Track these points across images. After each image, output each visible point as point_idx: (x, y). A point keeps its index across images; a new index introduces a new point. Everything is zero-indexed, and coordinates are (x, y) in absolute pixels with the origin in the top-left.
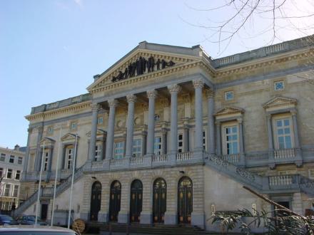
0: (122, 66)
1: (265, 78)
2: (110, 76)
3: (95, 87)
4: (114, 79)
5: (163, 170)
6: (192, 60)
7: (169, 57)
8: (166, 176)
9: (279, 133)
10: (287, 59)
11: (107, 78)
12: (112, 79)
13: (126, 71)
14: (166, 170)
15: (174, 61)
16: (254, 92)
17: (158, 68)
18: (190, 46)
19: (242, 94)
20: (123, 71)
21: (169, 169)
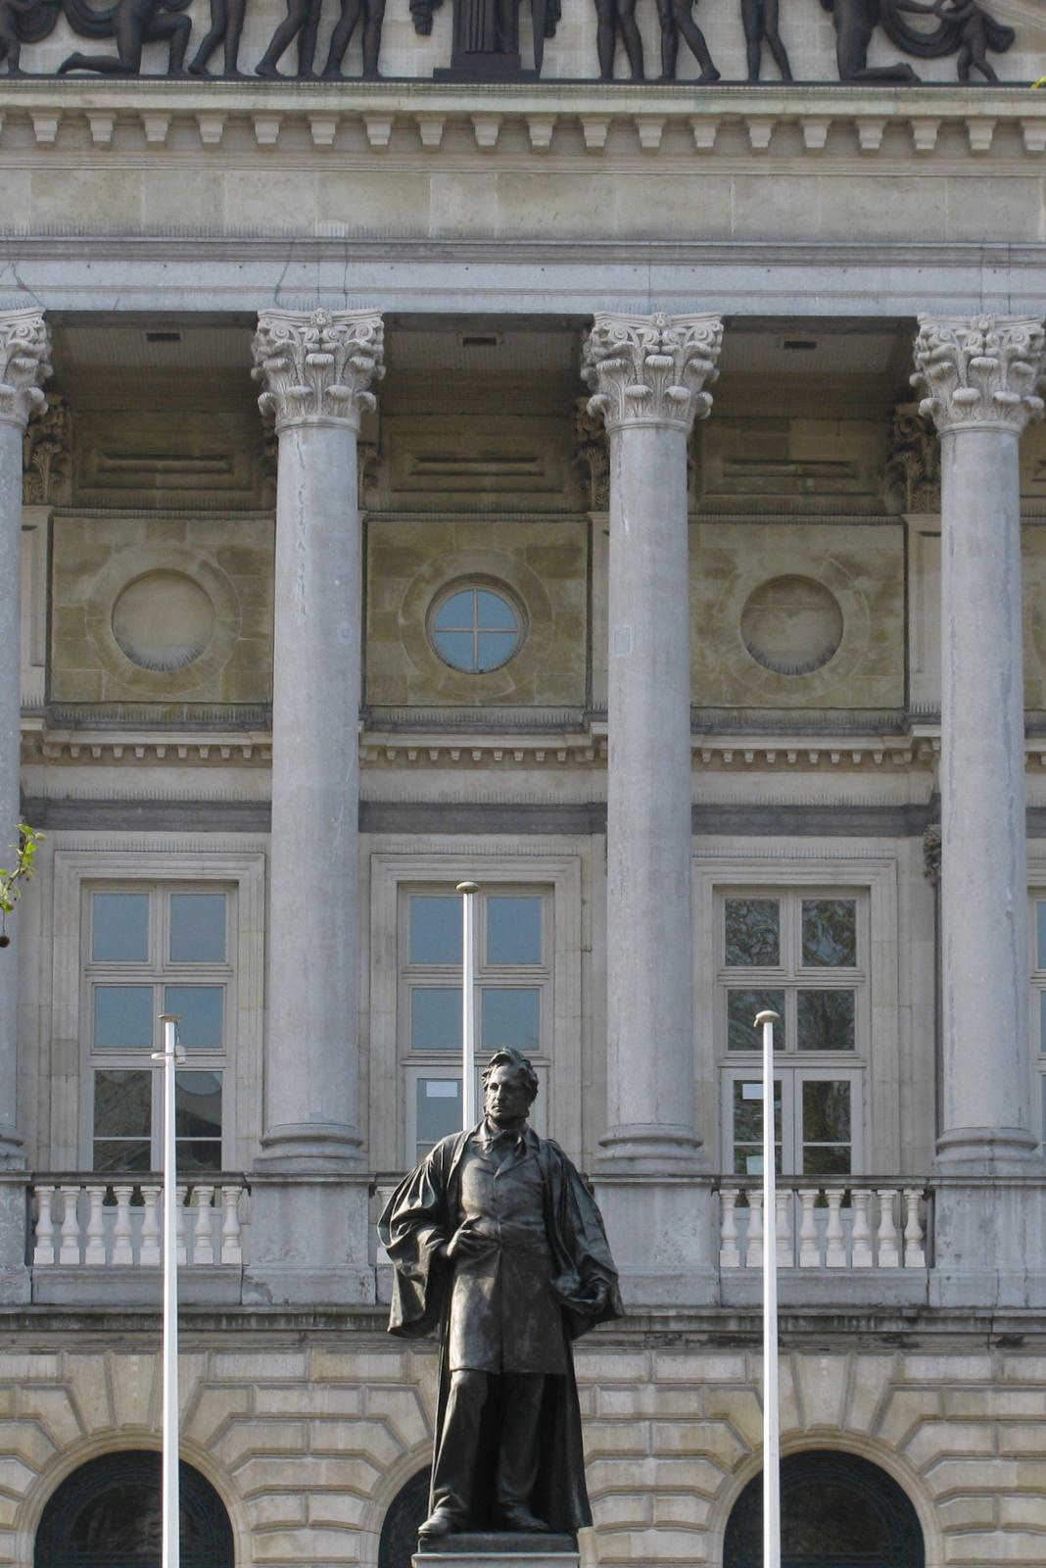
5: (874, 1370)
8: (934, 1438)
14: (919, 1367)
21: (975, 1367)
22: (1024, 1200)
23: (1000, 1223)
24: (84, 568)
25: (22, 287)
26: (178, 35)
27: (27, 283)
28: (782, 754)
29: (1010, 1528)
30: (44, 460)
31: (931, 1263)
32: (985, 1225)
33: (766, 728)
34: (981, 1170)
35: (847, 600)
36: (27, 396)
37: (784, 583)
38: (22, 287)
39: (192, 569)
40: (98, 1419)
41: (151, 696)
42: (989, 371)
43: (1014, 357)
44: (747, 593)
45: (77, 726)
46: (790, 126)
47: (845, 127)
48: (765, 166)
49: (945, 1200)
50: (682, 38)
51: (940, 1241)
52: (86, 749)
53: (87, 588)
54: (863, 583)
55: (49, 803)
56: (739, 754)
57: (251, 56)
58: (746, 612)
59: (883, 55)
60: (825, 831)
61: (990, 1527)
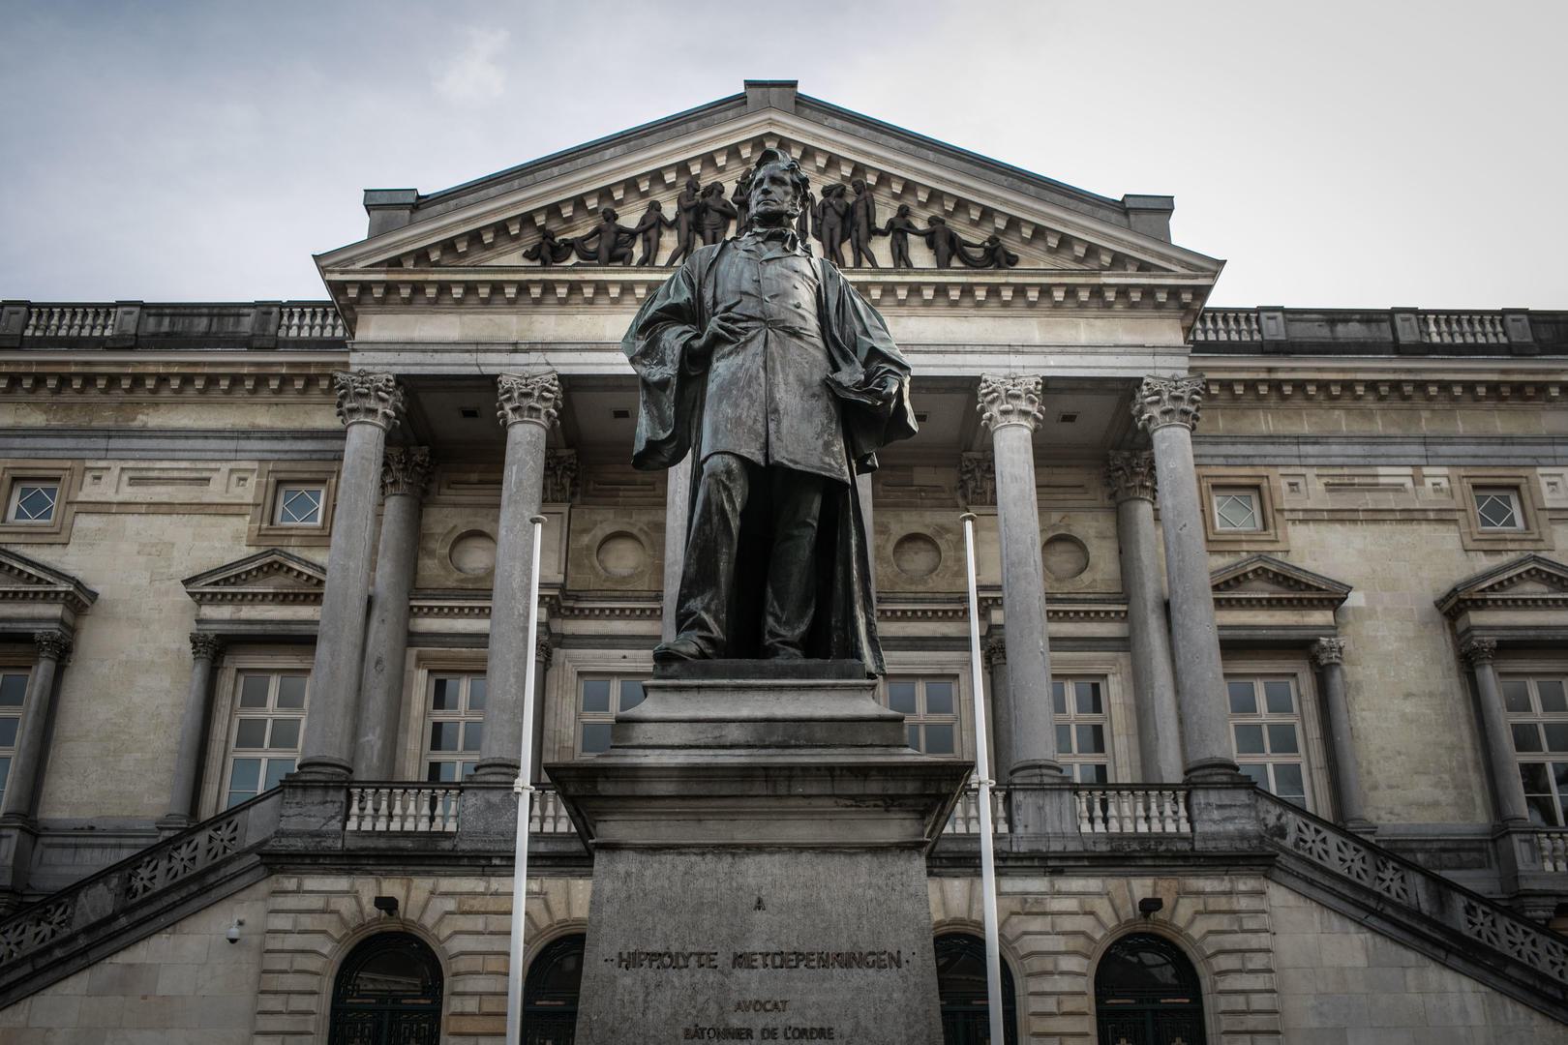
0: (631, 185)
1: (1430, 460)
2: (527, 219)
3: (395, 263)
4: (549, 252)
6: (1144, 267)
7: (987, 214)
9: (1521, 747)
10: (1542, 388)
11: (501, 228)
12: (531, 239)
13: (653, 224)
15: (1011, 244)
16: (1376, 516)
17: (900, 256)
18: (1113, 190)
19: (1310, 517)
20: (631, 218)
22: (1060, 796)
23: (1047, 809)
24: (585, 531)
25: (548, 364)
26: (627, 257)
27: (550, 361)
28: (914, 612)
29: (1062, 973)
30: (567, 482)
31: (1011, 830)
32: (1040, 808)
33: (907, 601)
34: (1036, 780)
35: (943, 546)
36: (548, 415)
37: (912, 538)
38: (548, 364)
39: (635, 531)
40: (560, 914)
41: (614, 587)
42: (1017, 397)
43: (1029, 392)
44: (896, 541)
45: (578, 599)
46: (915, 289)
47: (941, 290)
48: (903, 311)
49: (1018, 797)
50: (863, 256)
51: (1016, 818)
52: (582, 610)
53: (586, 539)
54: (949, 536)
55: (563, 636)
56: (894, 612)
57: (663, 259)
58: (895, 552)
59: (956, 263)
60: (936, 649)
61: (1051, 973)
